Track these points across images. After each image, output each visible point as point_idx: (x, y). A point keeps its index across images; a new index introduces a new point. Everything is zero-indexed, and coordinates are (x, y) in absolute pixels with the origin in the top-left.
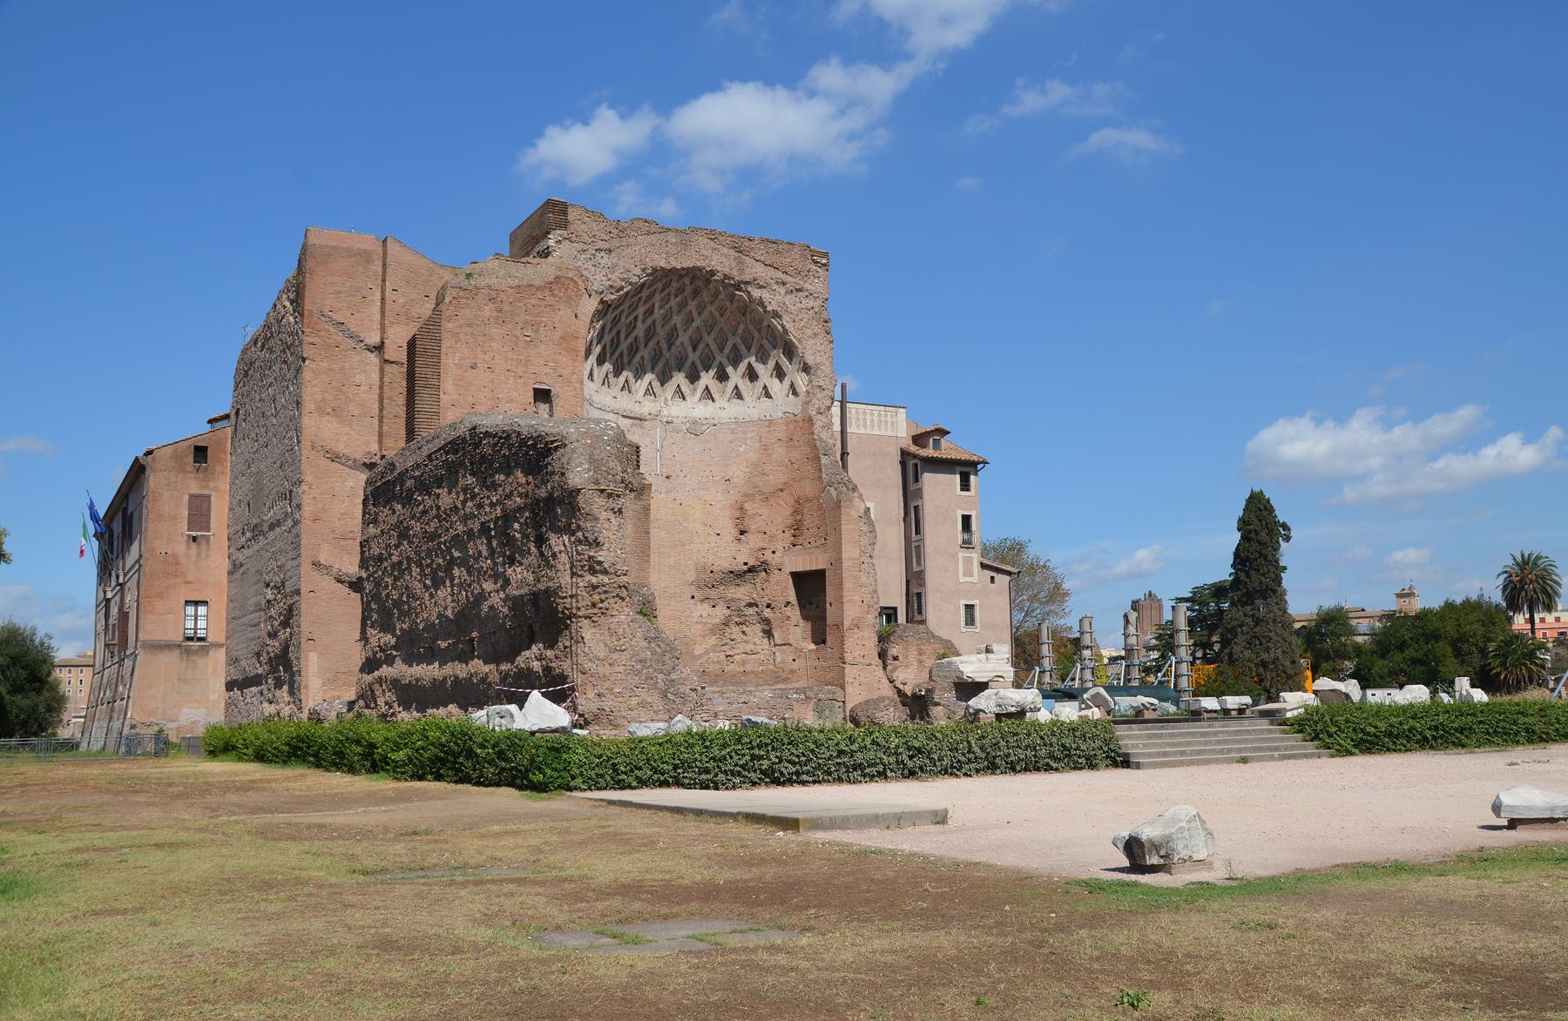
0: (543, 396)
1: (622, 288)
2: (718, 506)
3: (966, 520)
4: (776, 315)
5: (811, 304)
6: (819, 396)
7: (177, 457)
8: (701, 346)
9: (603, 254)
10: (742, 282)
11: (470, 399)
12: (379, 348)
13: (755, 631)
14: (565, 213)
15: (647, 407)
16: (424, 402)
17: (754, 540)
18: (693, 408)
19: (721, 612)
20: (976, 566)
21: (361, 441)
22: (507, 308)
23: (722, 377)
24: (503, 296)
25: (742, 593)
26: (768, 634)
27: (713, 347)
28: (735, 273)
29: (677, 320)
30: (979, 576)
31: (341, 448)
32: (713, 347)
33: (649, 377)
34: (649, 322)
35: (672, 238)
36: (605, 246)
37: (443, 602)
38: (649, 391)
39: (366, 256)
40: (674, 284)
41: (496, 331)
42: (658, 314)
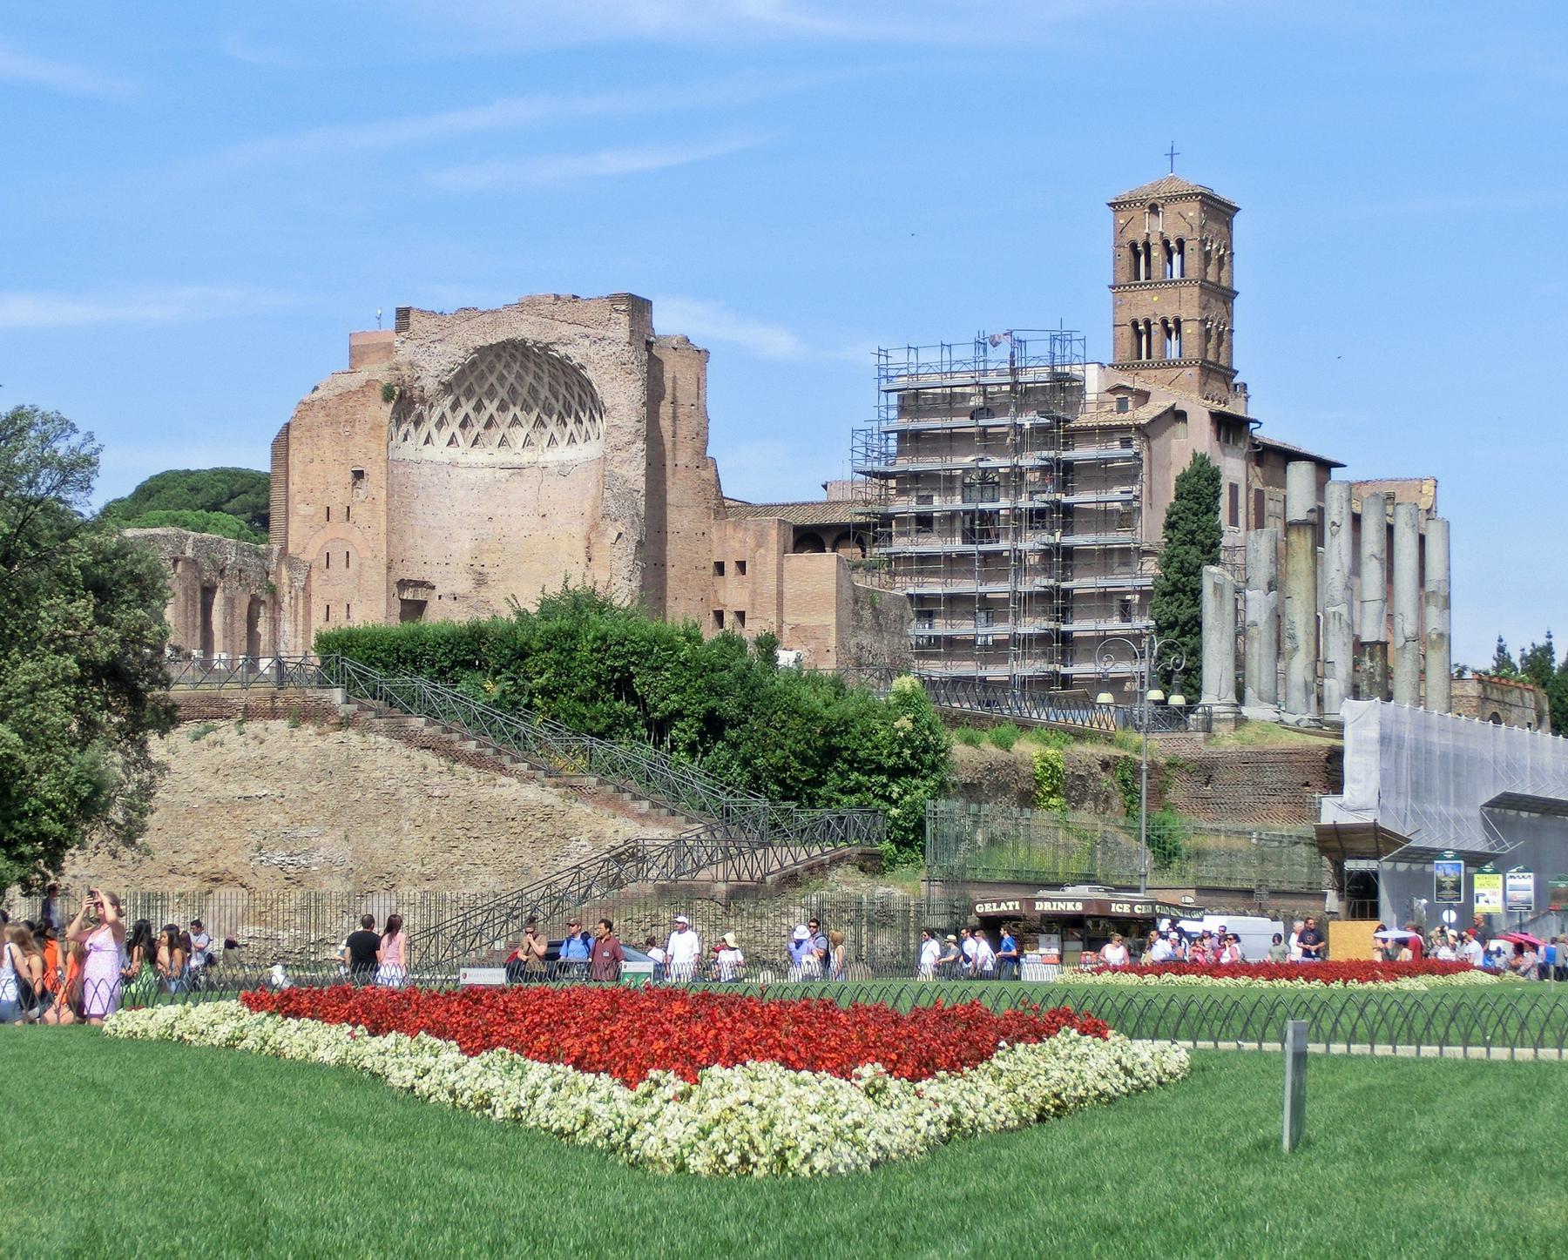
0: (359, 475)
1: (453, 369)
2: (577, 537)
4: (582, 367)
5: (614, 349)
6: (616, 434)
8: (561, 397)
9: (437, 344)
10: (547, 344)
11: (310, 486)
14: (408, 318)
15: (526, 457)
18: (563, 453)
22: (333, 412)
23: (579, 421)
24: (330, 404)
27: (568, 396)
28: (539, 339)
29: (529, 379)
32: (568, 396)
33: (527, 429)
34: (507, 385)
35: (488, 319)
36: (439, 337)
38: (527, 443)
40: (506, 356)
41: (326, 432)
42: (511, 379)
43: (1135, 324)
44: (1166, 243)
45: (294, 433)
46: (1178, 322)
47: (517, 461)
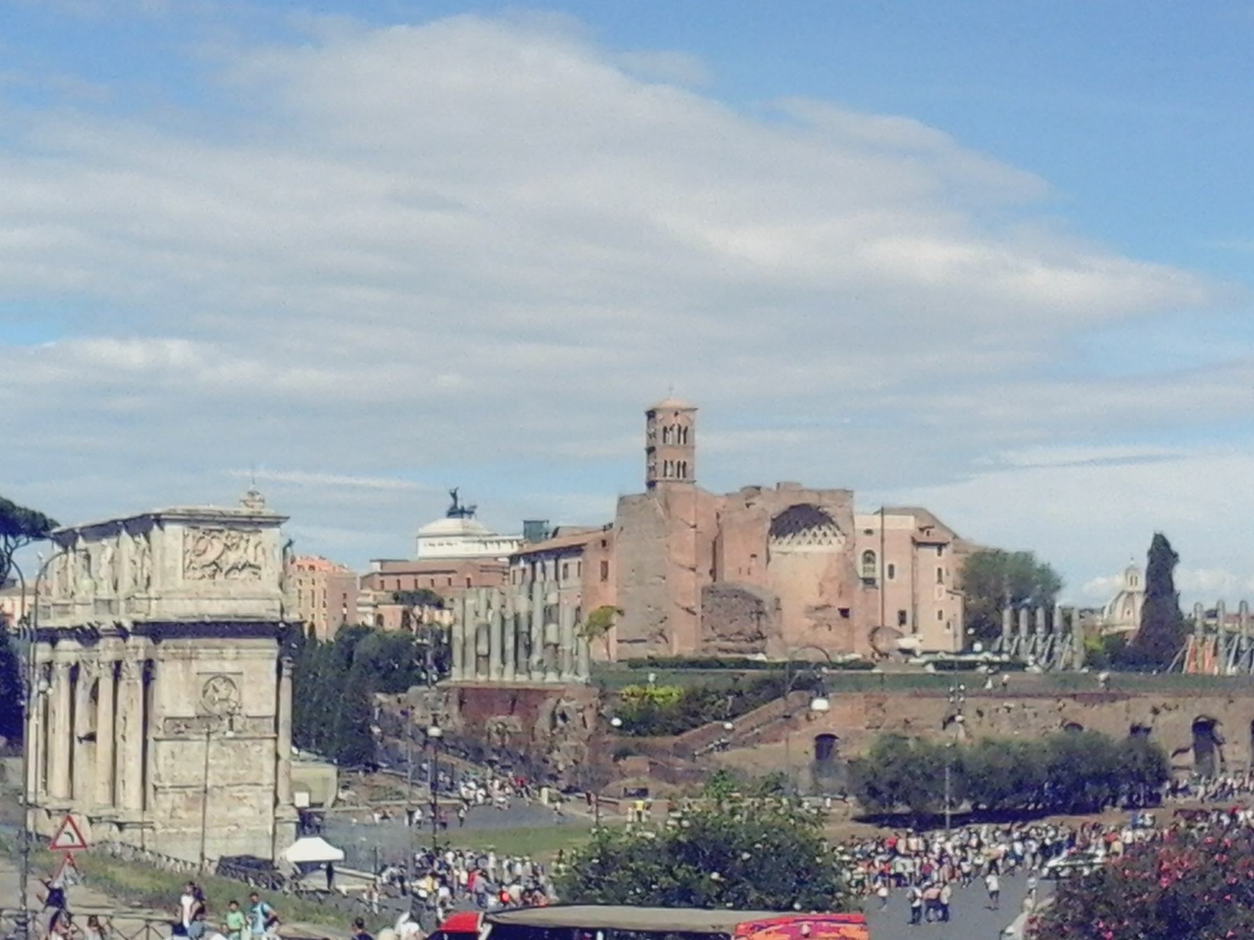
3: (940, 570)
7: (596, 545)
12: (695, 526)
13: (826, 628)
15: (788, 549)
16: (718, 557)
17: (825, 596)
18: (804, 548)
19: (813, 622)
20: (944, 591)
21: (689, 560)
25: (820, 614)
26: (830, 629)
30: (945, 597)
31: (683, 563)
37: (734, 627)
39: (690, 493)
43: (666, 462)
44: (680, 428)
45: (726, 535)
46: (685, 463)
47: (785, 550)
